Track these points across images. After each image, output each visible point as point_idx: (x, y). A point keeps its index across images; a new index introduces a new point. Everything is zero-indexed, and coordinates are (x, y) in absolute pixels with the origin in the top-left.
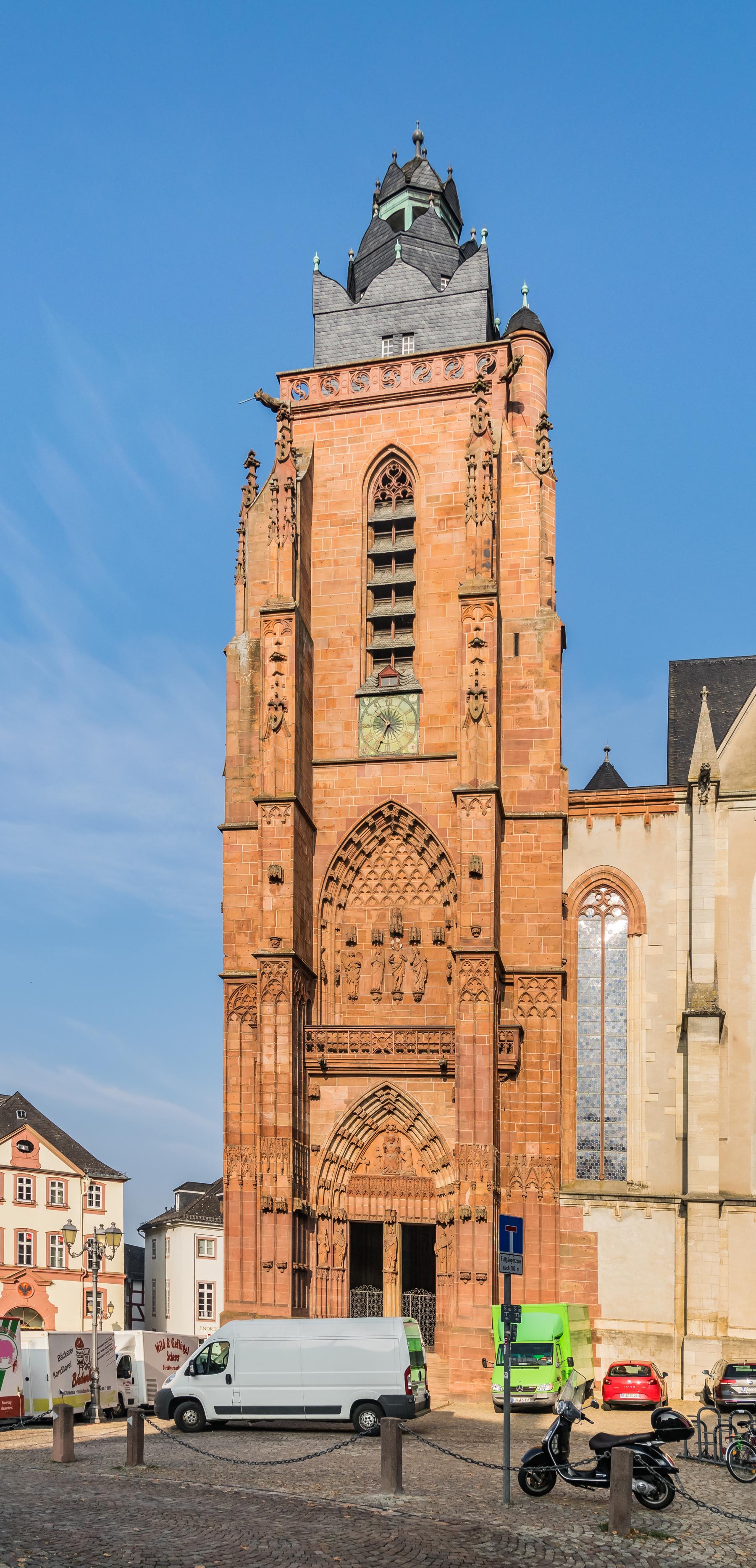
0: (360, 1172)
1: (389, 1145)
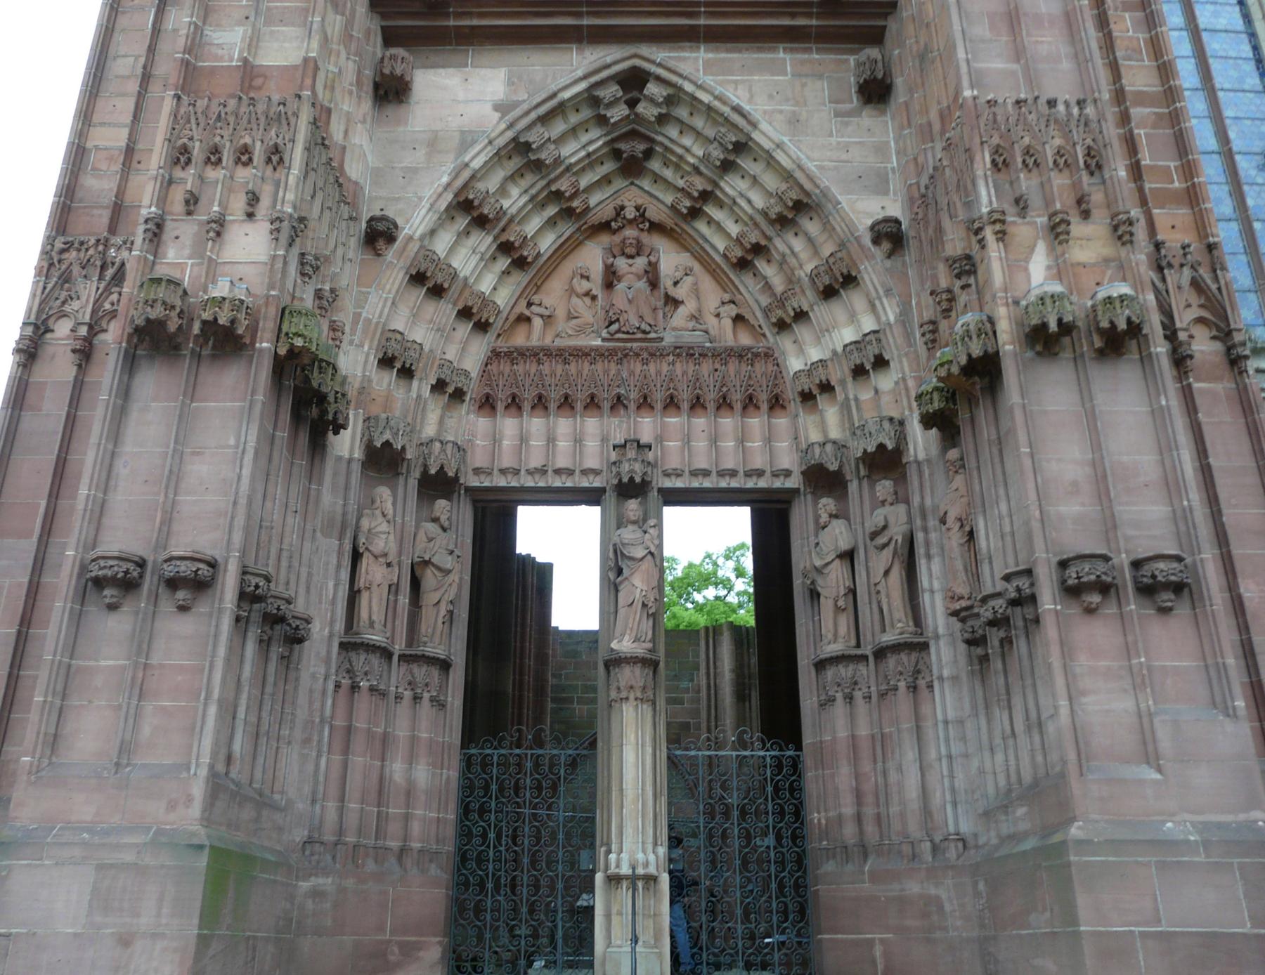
0: (519, 339)
1: (621, 263)
